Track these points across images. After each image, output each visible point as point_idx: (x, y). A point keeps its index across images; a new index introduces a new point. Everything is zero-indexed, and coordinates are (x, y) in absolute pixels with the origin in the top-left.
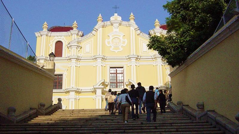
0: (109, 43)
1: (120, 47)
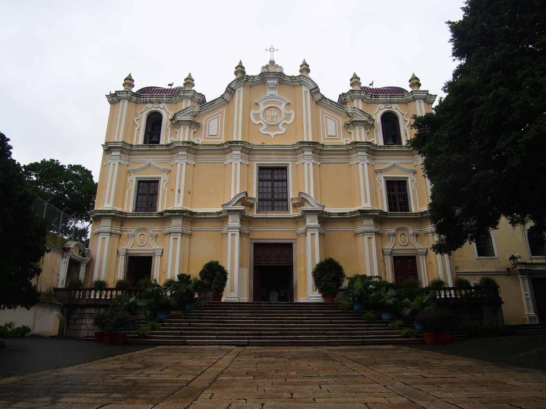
0: (257, 116)
1: (280, 126)
